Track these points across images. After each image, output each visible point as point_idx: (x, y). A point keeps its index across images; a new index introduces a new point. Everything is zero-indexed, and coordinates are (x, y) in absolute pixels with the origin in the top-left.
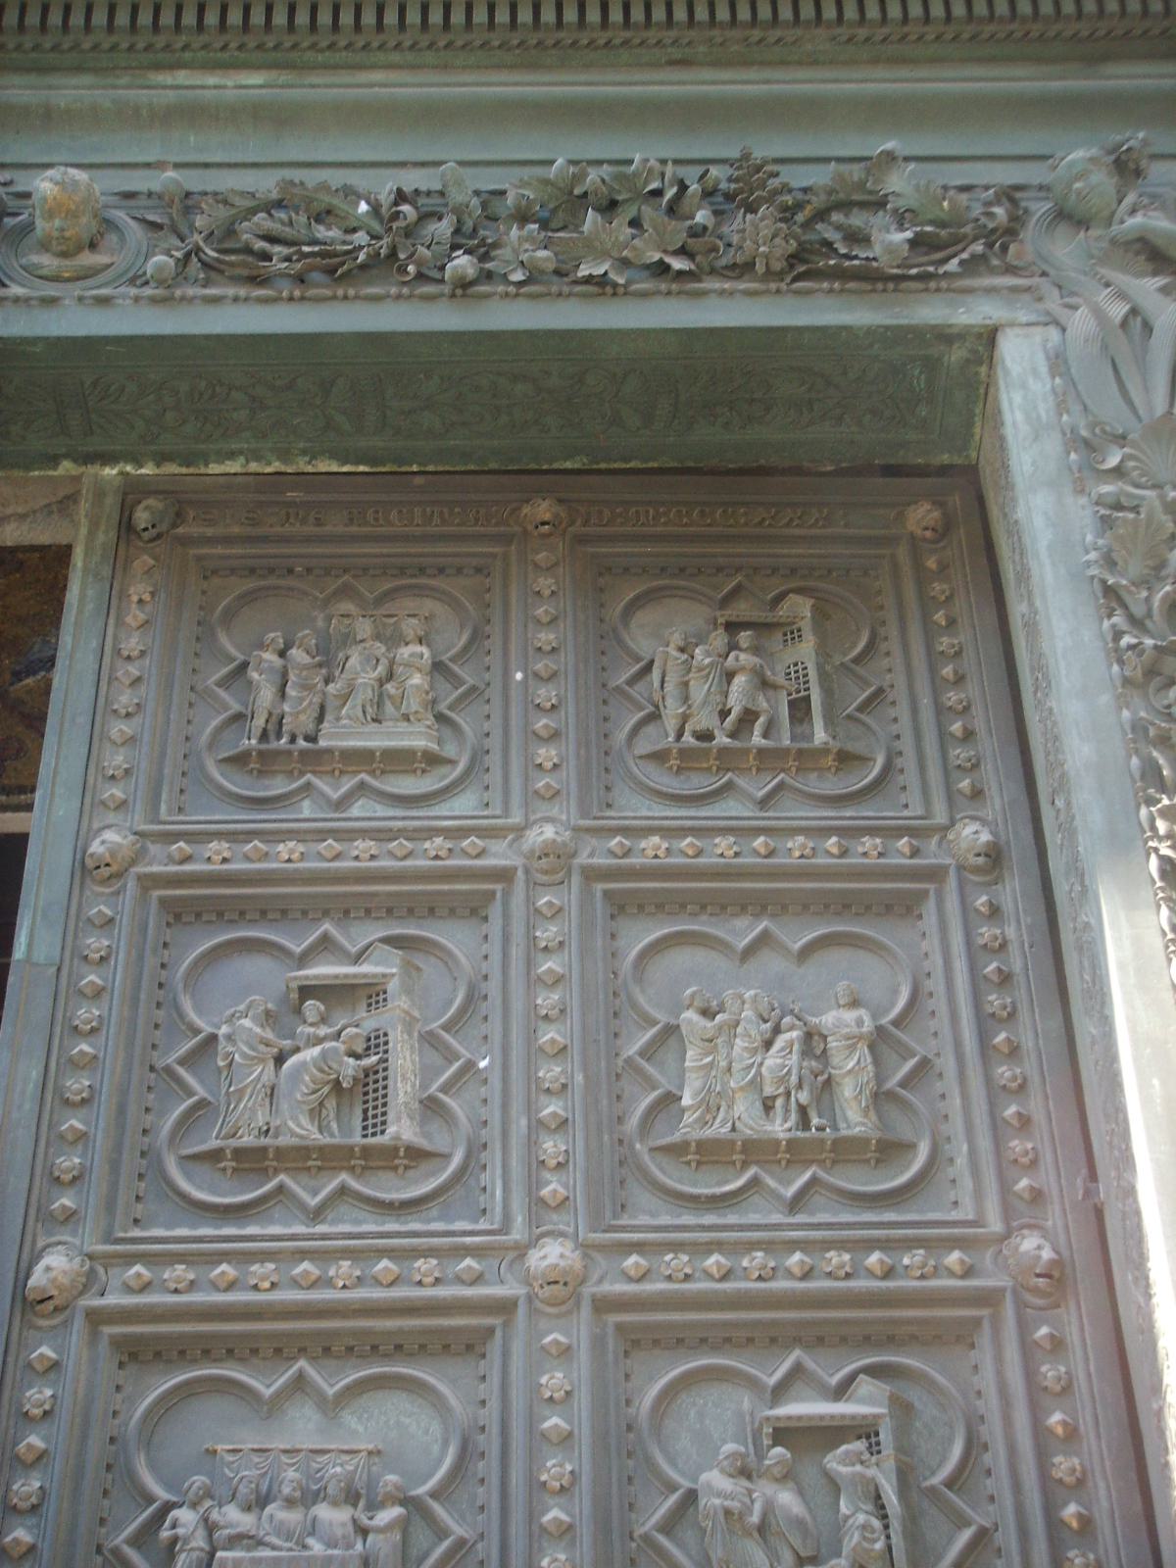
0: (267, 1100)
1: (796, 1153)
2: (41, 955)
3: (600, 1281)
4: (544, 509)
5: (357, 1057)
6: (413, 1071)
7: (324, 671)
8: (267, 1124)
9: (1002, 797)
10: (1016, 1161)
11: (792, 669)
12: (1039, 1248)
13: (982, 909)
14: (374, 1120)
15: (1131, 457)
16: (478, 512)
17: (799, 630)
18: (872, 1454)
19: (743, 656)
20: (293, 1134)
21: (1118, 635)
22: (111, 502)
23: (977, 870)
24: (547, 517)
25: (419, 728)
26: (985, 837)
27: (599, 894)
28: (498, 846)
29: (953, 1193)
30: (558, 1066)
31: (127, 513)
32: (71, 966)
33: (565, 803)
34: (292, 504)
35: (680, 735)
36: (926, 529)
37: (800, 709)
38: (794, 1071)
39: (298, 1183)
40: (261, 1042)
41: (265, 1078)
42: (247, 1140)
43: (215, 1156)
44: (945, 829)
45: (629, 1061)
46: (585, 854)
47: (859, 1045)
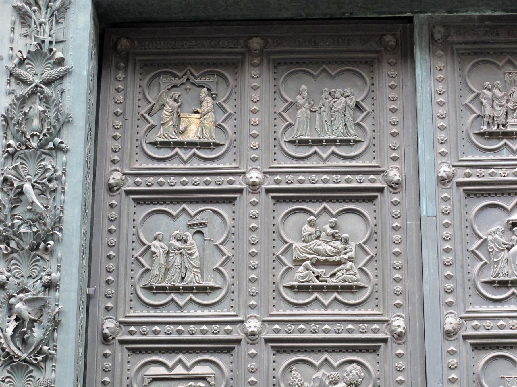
0: (507, 264)
2: (430, 214)
7: (505, 98)
8: (508, 272)
22: (426, 28)
31: (431, 33)
32: (439, 215)
34: (487, 26)
40: (503, 244)
41: (505, 257)
42: (503, 278)
43: (491, 283)
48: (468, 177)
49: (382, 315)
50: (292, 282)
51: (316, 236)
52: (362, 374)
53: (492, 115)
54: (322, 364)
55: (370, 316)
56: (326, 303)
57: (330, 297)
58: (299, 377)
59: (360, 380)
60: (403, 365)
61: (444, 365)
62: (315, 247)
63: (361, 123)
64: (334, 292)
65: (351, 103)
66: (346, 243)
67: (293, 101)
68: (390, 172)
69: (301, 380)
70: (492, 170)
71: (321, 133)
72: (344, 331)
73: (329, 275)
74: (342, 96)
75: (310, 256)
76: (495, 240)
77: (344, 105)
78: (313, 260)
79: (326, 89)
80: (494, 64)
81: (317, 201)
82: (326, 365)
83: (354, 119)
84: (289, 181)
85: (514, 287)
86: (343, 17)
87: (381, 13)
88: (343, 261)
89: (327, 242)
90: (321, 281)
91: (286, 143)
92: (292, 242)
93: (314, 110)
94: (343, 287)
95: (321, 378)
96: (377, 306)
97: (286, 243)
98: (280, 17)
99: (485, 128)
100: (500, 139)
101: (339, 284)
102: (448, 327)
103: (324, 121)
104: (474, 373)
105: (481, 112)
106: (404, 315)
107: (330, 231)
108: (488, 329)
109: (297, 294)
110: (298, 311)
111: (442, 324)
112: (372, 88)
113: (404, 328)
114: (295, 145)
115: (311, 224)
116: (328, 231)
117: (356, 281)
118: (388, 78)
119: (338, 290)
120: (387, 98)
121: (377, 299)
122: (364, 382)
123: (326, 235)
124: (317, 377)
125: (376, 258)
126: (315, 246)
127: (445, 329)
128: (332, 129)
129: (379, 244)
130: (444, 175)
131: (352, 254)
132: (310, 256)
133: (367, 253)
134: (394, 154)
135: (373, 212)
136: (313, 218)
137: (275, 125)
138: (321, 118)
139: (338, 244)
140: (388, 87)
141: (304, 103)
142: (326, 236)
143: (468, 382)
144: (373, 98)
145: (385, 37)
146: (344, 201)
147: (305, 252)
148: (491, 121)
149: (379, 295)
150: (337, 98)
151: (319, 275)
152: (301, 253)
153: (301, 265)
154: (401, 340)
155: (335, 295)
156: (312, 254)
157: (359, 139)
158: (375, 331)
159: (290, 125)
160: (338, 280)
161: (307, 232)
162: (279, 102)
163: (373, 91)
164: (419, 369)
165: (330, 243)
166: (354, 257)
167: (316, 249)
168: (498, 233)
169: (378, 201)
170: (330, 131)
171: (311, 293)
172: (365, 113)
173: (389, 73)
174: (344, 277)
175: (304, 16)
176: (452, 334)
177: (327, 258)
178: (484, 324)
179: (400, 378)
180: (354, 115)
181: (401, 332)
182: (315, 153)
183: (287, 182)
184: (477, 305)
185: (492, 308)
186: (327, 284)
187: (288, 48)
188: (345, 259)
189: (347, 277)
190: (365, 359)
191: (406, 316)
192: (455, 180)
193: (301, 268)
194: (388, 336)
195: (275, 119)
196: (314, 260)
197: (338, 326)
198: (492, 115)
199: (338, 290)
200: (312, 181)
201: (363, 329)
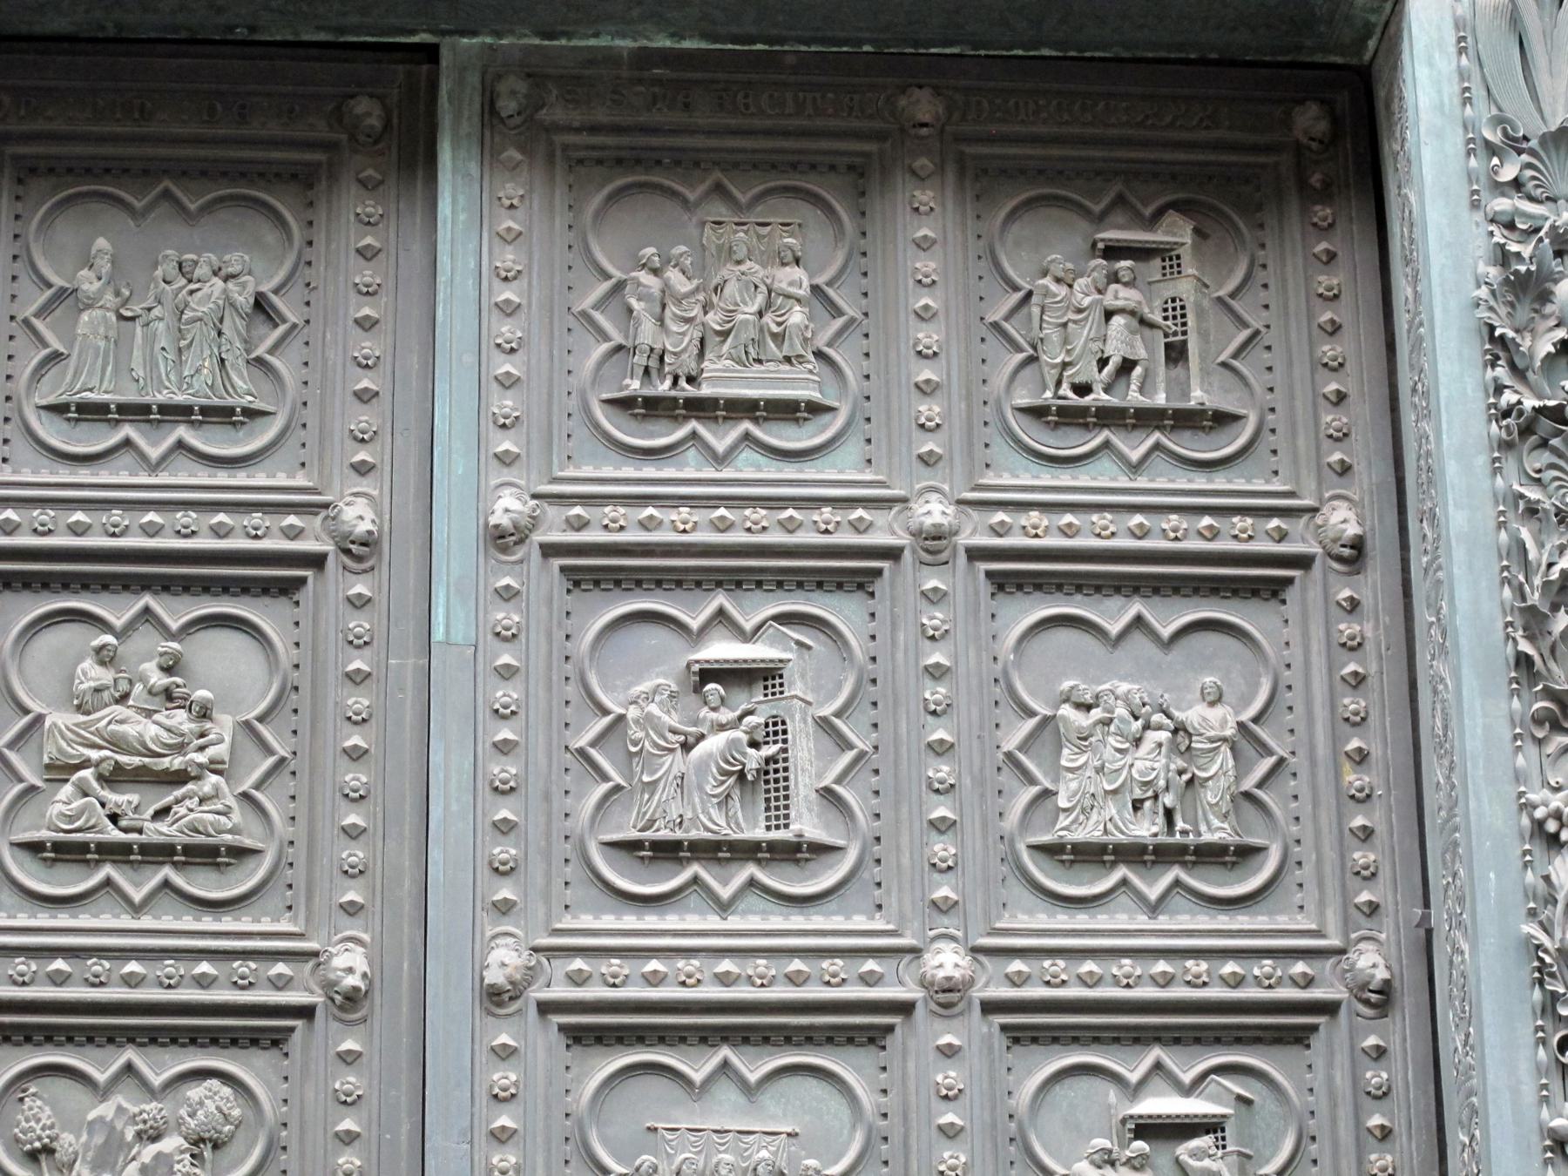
0: (679, 791)
1: (1164, 855)
2: (458, 636)
3: (987, 985)
4: (924, 106)
5: (754, 744)
6: (810, 761)
7: (701, 297)
8: (681, 816)
9: (1371, 478)
10: (1358, 873)
11: (1170, 305)
12: (1374, 966)
13: (1344, 604)
14: (779, 812)
15: (1529, 166)
16: (852, 99)
17: (1178, 257)
18: (1217, 1147)
19: (1125, 293)
20: (707, 829)
21: (1499, 389)
22: (474, 79)
23: (1340, 559)
24: (927, 118)
25: (798, 372)
26: (1352, 530)
27: (982, 576)
28: (880, 518)
29: (1299, 895)
30: (945, 764)
31: (488, 94)
32: (485, 641)
33: (947, 471)
34: (658, 81)
35: (1059, 384)
36: (1312, 139)
37: (1176, 353)
38: (1162, 775)
39: (709, 872)
40: (670, 731)
41: (675, 771)
42: (664, 834)
44: (1314, 510)
45: (1009, 755)
46: (968, 532)
47: (1223, 749)
48: (578, 530)
49: (303, 935)
50: (38, 829)
51: (117, 695)
52: (236, 1112)
53: (658, 346)
54: (116, 1079)
55: (265, 939)
56: (137, 896)
57: (150, 879)
58: (46, 1116)
59: (227, 1128)
60: (357, 1088)
61: (477, 1088)
62: (112, 727)
63: (268, 357)
64: (163, 863)
65: (241, 299)
66: (204, 716)
67: (67, 285)
68: (345, 508)
69: (52, 1127)
70: (650, 511)
71: (146, 384)
72: (184, 982)
73: (151, 811)
74: (215, 274)
75: (94, 755)
76: (648, 721)
77: (221, 302)
78: (104, 765)
79: (169, 252)
80: (674, 194)
81: (126, 588)
82: (130, 1082)
83: (249, 345)
84: (43, 525)
85: (698, 859)
86: (230, 37)
87: (341, 30)
88: (193, 772)
89: (149, 714)
90: (125, 830)
91: (42, 413)
92: (44, 712)
93: (129, 314)
94: (189, 850)
95: (112, 1120)
96: (290, 908)
97: (26, 711)
98: (38, 29)
99: (635, 386)
100: (678, 420)
101: (177, 840)
102: (494, 976)
103: (157, 347)
104: (567, 1115)
105: (626, 337)
106: (366, 937)
107: (158, 679)
108: (614, 985)
109: (50, 867)
110: (51, 917)
111: (477, 967)
112: (309, 254)
113: (365, 975)
114: (69, 420)
115: (104, 657)
116: (152, 681)
117: (230, 831)
118: (354, 227)
119: (176, 858)
120: (350, 285)
121: (290, 886)
122: (240, 1135)
123: (145, 692)
124: (101, 1119)
125: (292, 766)
126: (110, 723)
127: (487, 981)
128: (181, 373)
129: (303, 721)
130: (505, 521)
131: (220, 751)
132: (94, 755)
133: (268, 750)
134: (362, 455)
135: (292, 626)
136: (109, 639)
137: (10, 357)
138: (150, 340)
139: (180, 719)
140: (353, 253)
141: (101, 292)
142: (145, 695)
143: (548, 1141)
144: (308, 285)
145: (352, 102)
146: (206, 590)
147: (79, 740)
148: (653, 363)
149: (298, 875)
150: (199, 281)
151: (119, 812)
152: (69, 745)
153: (66, 781)
154: (355, 1011)
155: (167, 871)
156: (101, 748)
157: (259, 405)
158: (280, 984)
159: (56, 357)
160: (175, 826)
161: (88, 680)
162: (26, 284)
163: (309, 263)
164: (403, 1098)
165: (156, 717)
166: (227, 759)
167: (113, 733)
168: (657, 698)
169: (306, 595)
170: (172, 378)
171: (92, 865)
172: (282, 329)
173: (359, 210)
174: (195, 819)
175: (111, 32)
176: (506, 997)
177: (147, 760)
178: (604, 970)
179: (348, 1124)
180: (248, 331)
181: (356, 989)
182: (127, 443)
183: (35, 530)
184: (587, 911)
185: (630, 921)
186: (143, 838)
187: (59, 126)
188: (200, 766)
189: (201, 821)
190: (247, 1065)
191: (373, 939)
192: (538, 537)
193: (67, 790)
194: (317, 998)
195: (11, 338)
196: (107, 768)
197: (169, 967)
198: (658, 346)
199: (176, 858)
200: (112, 529)
201: (243, 978)
